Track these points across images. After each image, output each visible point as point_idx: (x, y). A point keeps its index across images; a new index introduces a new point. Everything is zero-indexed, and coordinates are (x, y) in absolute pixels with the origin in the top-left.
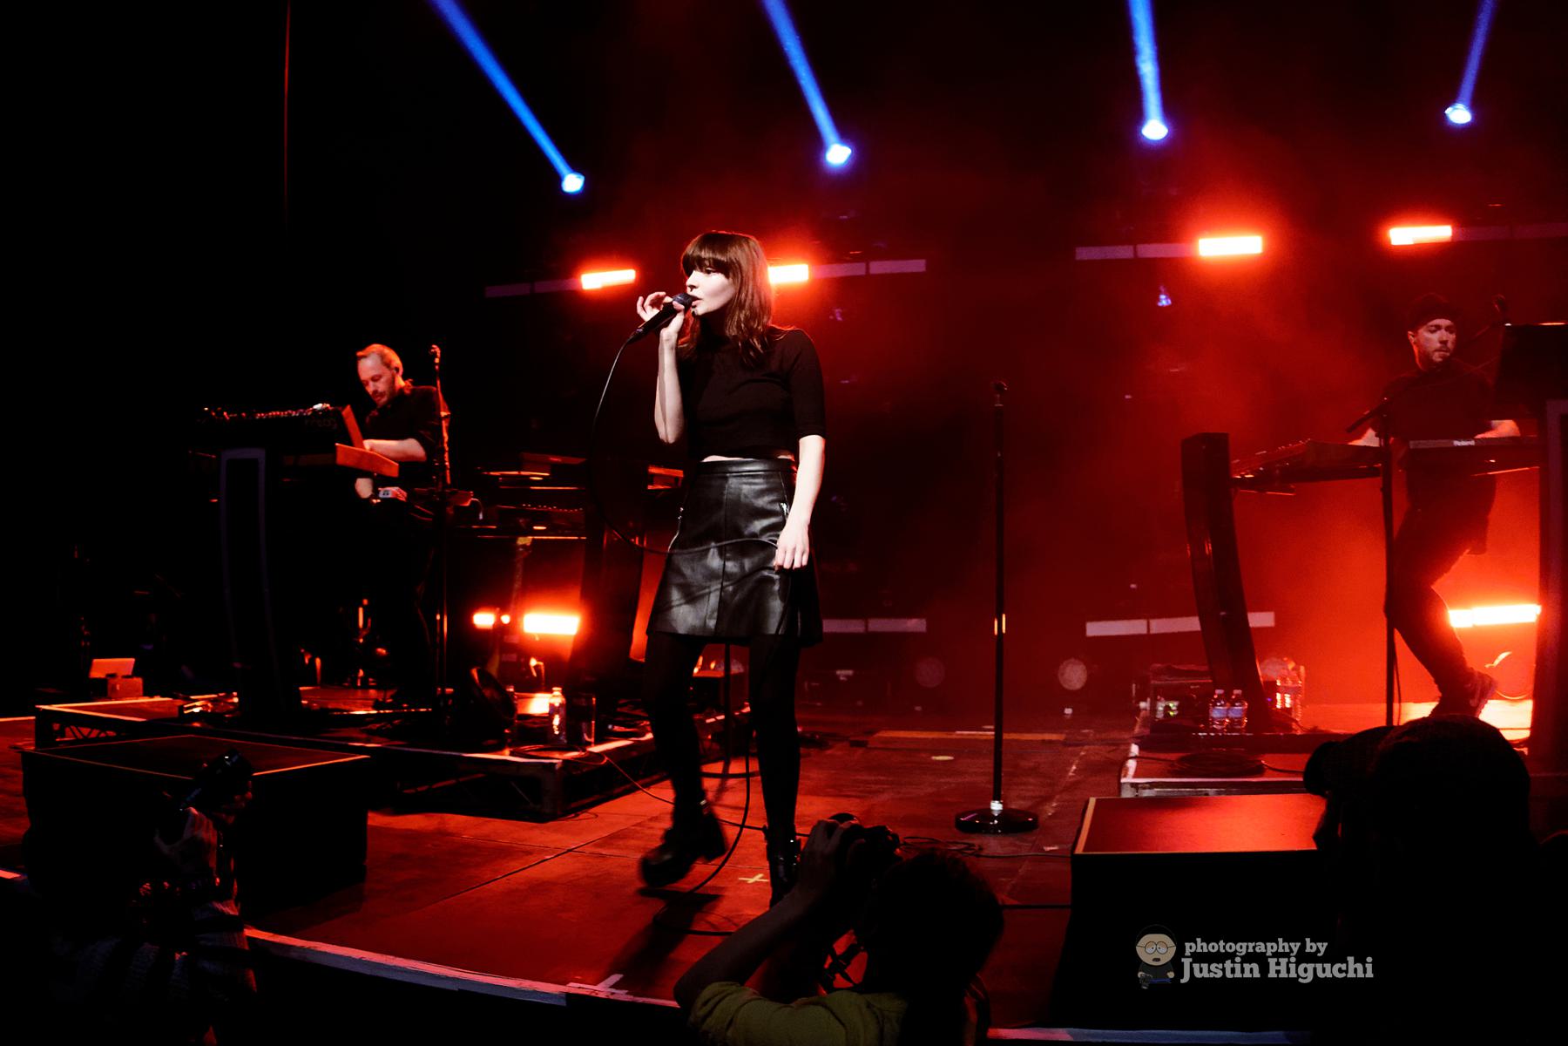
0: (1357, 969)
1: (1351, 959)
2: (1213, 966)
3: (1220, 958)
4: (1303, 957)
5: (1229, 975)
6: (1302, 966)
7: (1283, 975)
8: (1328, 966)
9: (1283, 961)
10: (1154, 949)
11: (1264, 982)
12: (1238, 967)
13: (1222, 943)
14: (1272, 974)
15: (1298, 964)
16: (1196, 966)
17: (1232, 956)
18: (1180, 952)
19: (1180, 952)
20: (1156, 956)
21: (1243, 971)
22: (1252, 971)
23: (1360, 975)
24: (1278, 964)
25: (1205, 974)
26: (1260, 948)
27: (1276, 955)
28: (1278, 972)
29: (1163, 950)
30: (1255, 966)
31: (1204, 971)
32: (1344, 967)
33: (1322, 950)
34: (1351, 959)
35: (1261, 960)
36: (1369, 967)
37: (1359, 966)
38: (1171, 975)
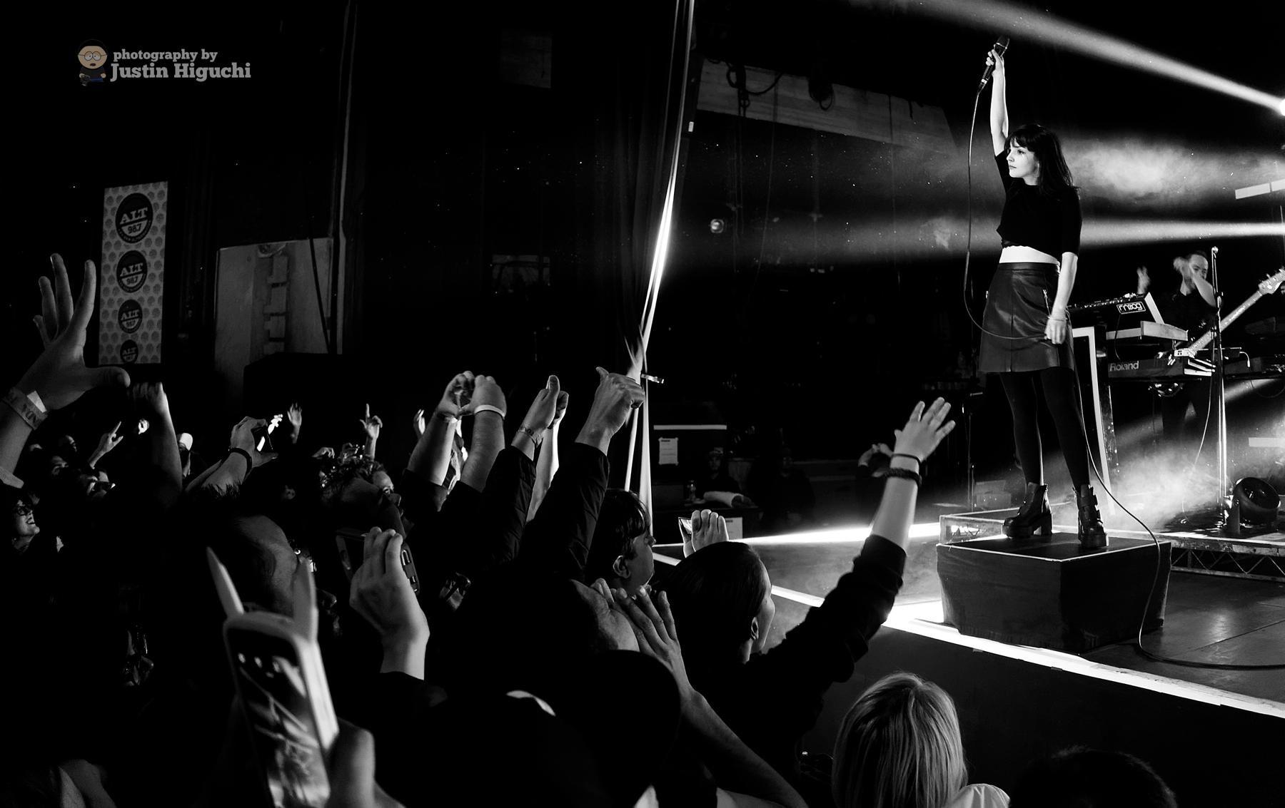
0: (239, 72)
1: (234, 64)
2: (134, 69)
3: (139, 63)
4: (200, 63)
5: (146, 76)
6: (199, 70)
7: (185, 75)
8: (217, 69)
9: (186, 66)
10: (91, 56)
11: (172, 83)
12: (152, 70)
14: (177, 75)
15: (195, 68)
16: (122, 69)
17: (148, 62)
18: (110, 59)
19: (110, 59)
22: (163, 73)
23: (242, 76)
25: (128, 75)
26: (169, 56)
27: (180, 61)
29: (97, 57)
30: (165, 69)
31: (127, 73)
34: (234, 64)
35: (169, 65)
36: (248, 70)
37: (241, 69)
38: (104, 76)
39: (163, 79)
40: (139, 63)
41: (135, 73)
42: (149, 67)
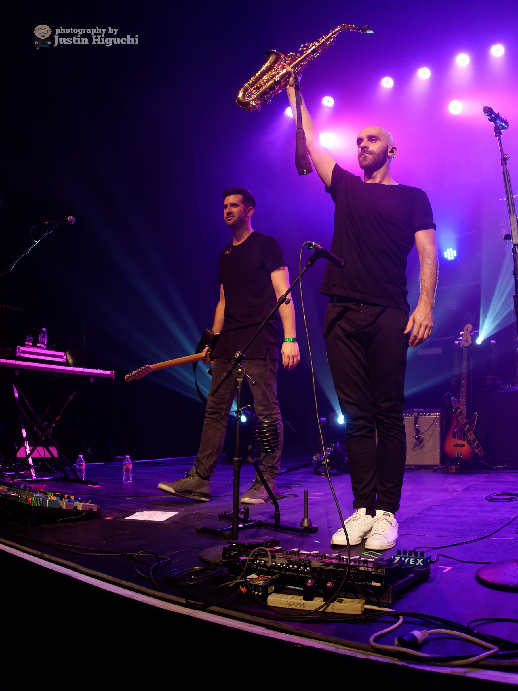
0: (131, 40)
1: (128, 36)
2: (68, 39)
3: (71, 35)
5: (75, 43)
6: (107, 39)
7: (99, 43)
8: (118, 39)
9: (99, 37)
10: (42, 31)
12: (79, 39)
13: (72, 29)
14: (94, 43)
16: (60, 39)
17: (76, 35)
18: (53, 33)
19: (53, 33)
20: (43, 34)
21: (81, 41)
22: (85, 41)
23: (133, 43)
24: (96, 38)
25: (64, 43)
26: (89, 31)
27: (96, 34)
28: (96, 42)
29: (46, 32)
30: (86, 39)
31: (64, 41)
32: (125, 39)
33: (116, 32)
34: (128, 36)
36: (137, 39)
37: (132, 39)
38: (49, 43)
39: (85, 45)
40: (71, 35)
41: (68, 41)
42: (77, 37)
